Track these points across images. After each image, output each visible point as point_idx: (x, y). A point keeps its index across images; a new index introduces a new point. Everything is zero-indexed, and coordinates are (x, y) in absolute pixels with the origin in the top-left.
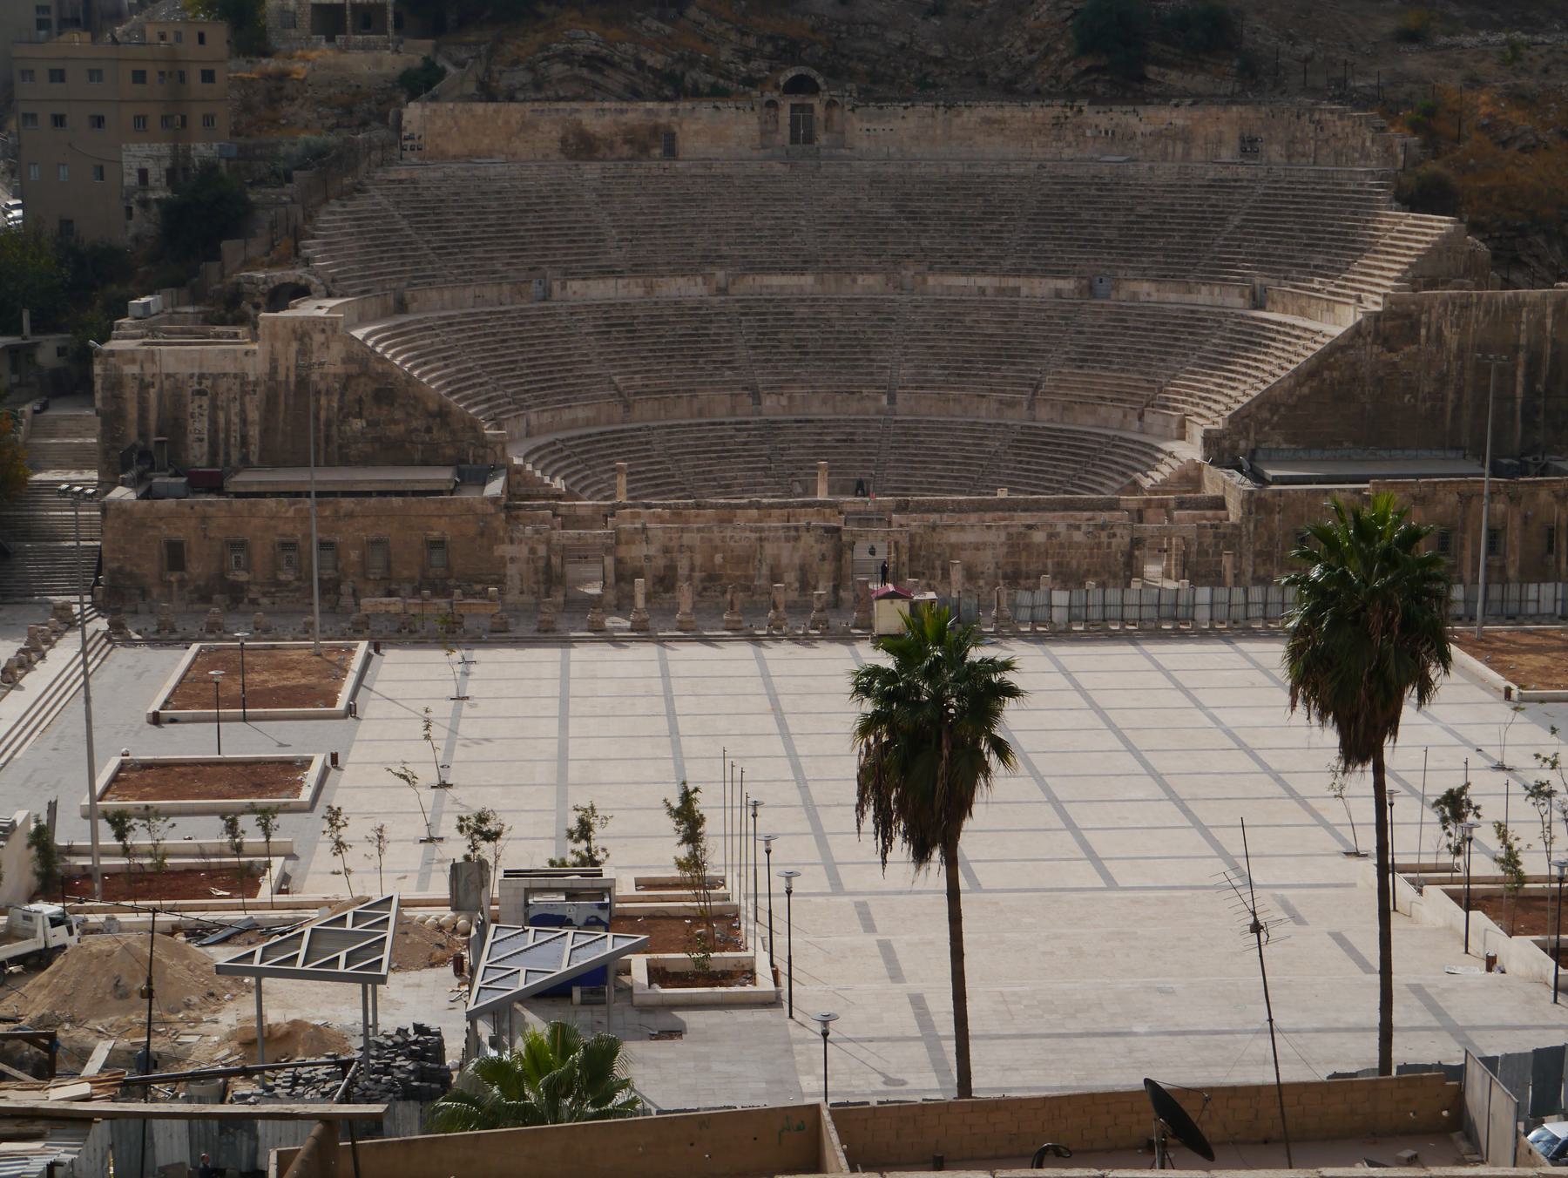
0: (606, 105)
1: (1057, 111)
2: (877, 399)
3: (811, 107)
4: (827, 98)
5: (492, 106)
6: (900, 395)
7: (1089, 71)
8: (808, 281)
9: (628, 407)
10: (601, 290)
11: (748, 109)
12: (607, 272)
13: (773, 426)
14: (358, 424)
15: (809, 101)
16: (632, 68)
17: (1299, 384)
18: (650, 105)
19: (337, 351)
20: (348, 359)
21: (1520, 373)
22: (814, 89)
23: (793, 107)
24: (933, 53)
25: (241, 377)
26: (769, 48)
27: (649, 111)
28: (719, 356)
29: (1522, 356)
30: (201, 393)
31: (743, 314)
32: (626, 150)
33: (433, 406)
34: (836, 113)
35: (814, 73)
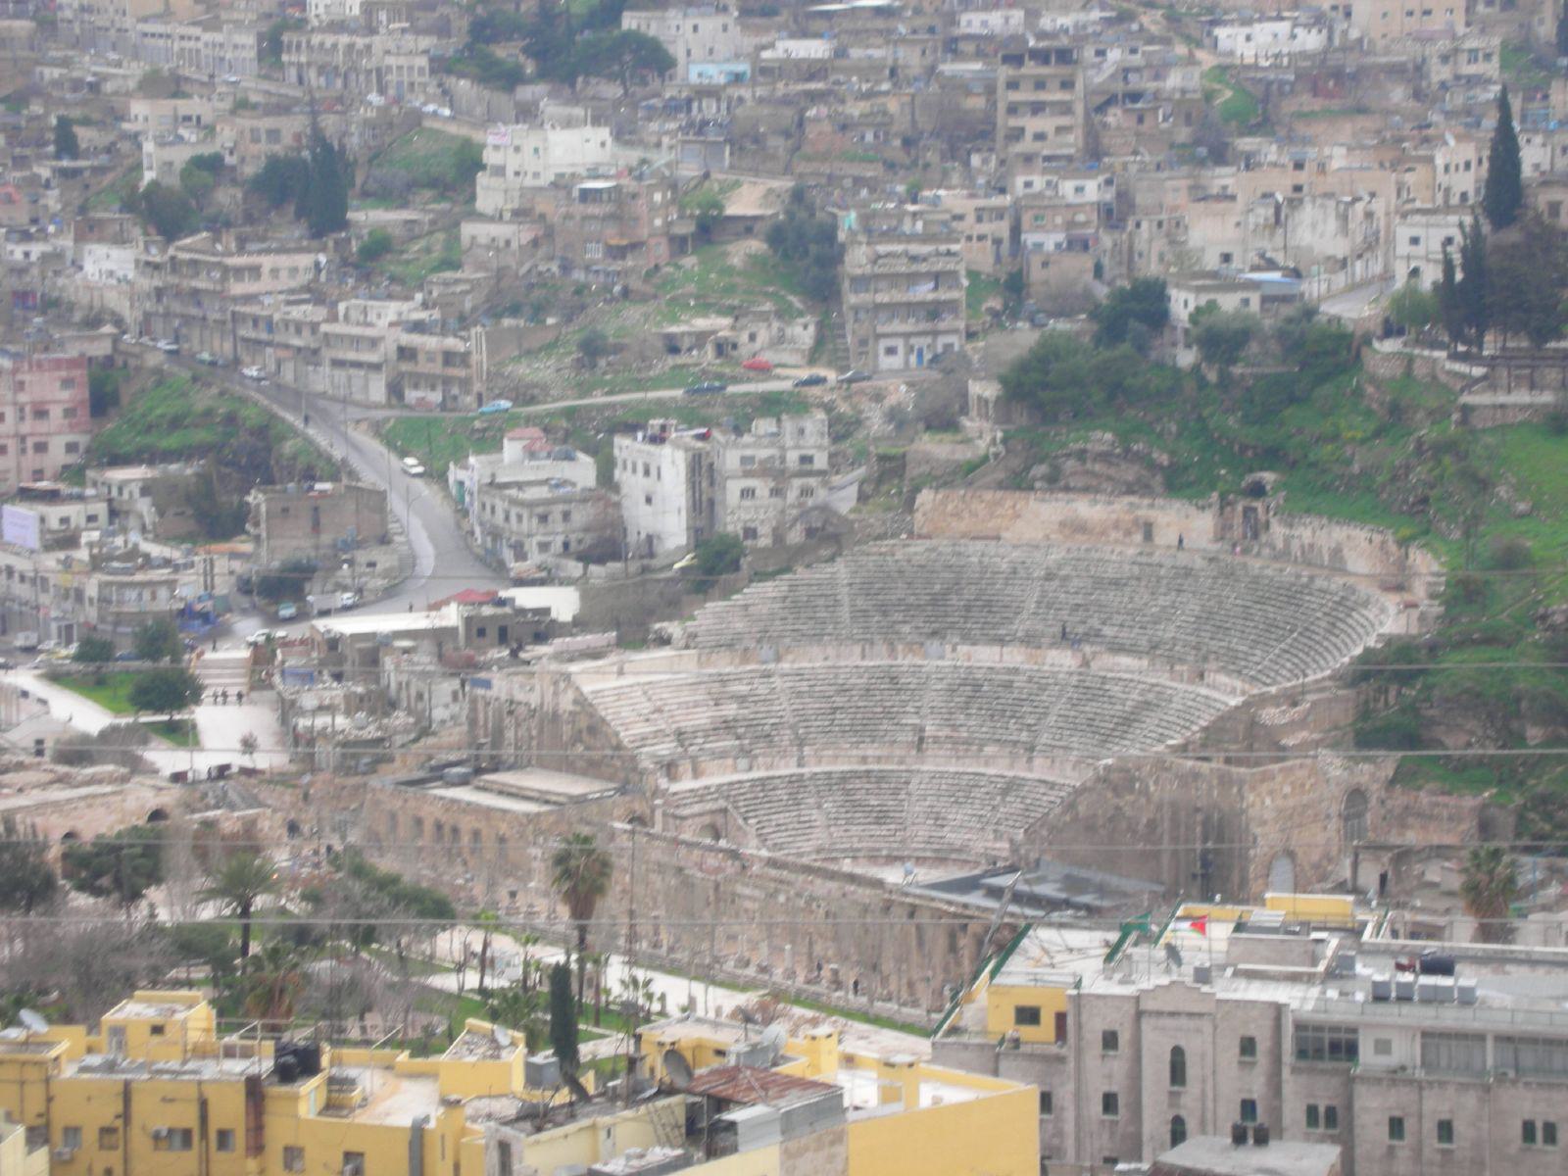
3: (1255, 510)
5: (999, 494)
8: (1145, 662)
9: (919, 749)
10: (986, 656)
12: (1001, 641)
14: (580, 748)
17: (1064, 813)
19: (570, 695)
20: (576, 702)
21: (1199, 829)
25: (527, 704)
27: (1131, 504)
29: (1199, 817)
30: (511, 713)
32: (1114, 535)
33: (614, 742)
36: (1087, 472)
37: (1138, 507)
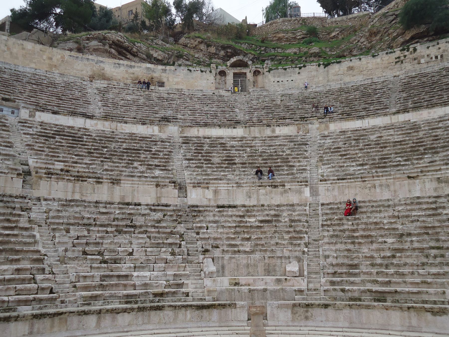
0: (121, 62)
1: (398, 53)
2: (300, 192)
4: (254, 69)
6: (322, 188)
7: (412, 38)
11: (208, 72)
13: (196, 210)
15: (244, 70)
16: (144, 56)
18: (149, 65)
22: (245, 65)
23: (236, 75)
24: (312, 51)
26: (222, 53)
27: (149, 68)
28: (156, 162)
31: (184, 143)
34: (260, 78)
35: (246, 59)
36: (106, 51)
37: (153, 71)
